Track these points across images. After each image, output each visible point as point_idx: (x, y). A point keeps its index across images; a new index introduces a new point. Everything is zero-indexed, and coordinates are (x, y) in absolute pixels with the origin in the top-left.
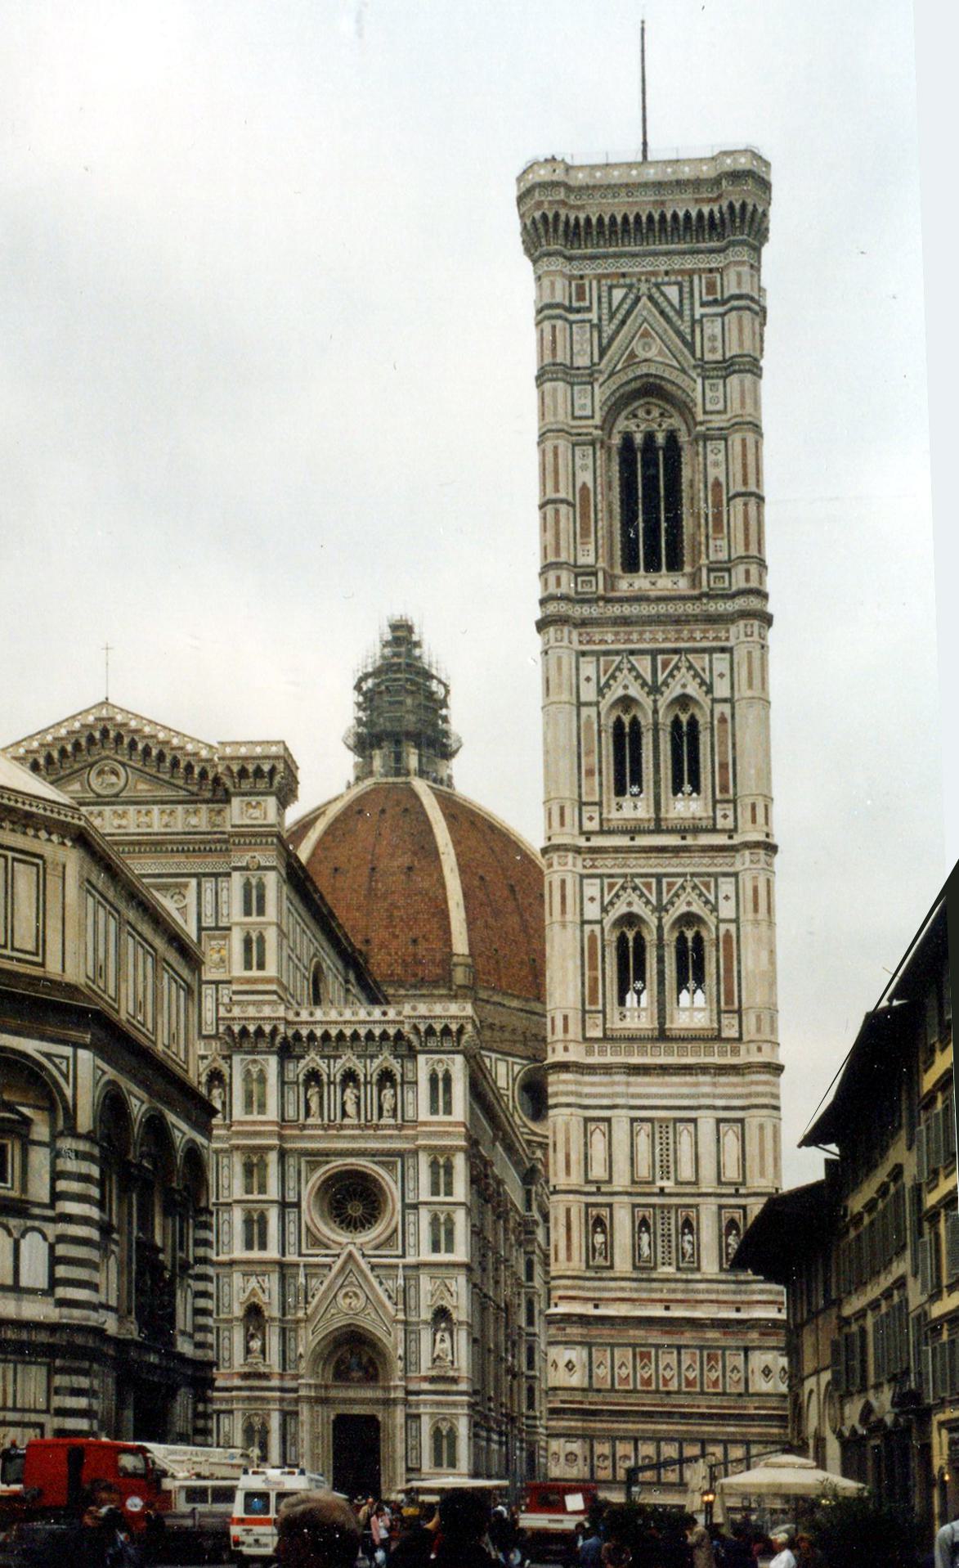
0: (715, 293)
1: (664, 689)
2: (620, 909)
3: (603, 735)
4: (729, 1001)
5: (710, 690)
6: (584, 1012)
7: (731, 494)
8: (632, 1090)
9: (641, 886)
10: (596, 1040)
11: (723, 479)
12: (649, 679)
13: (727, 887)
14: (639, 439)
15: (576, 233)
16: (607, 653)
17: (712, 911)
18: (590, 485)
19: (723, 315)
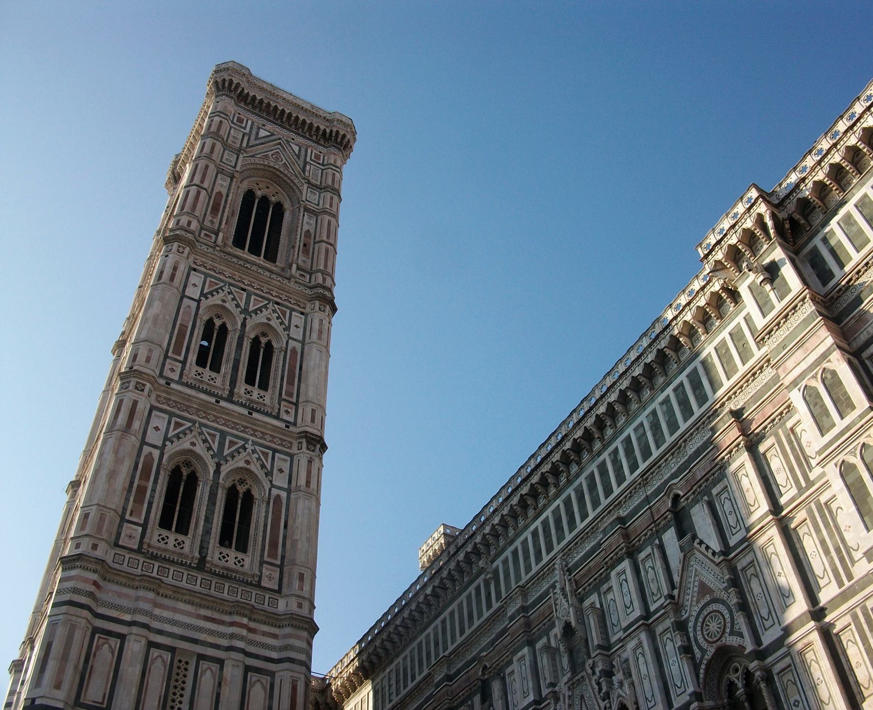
0: (319, 160)
1: (253, 315)
2: (185, 444)
3: (198, 320)
4: (273, 555)
5: (287, 329)
6: (123, 519)
7: (317, 239)
8: (157, 611)
9: (206, 433)
10: (131, 550)
11: (312, 231)
12: (242, 305)
13: (281, 462)
14: (259, 193)
15: (243, 98)
16: (211, 276)
17: (267, 474)
18: (224, 193)
19: (323, 170)
